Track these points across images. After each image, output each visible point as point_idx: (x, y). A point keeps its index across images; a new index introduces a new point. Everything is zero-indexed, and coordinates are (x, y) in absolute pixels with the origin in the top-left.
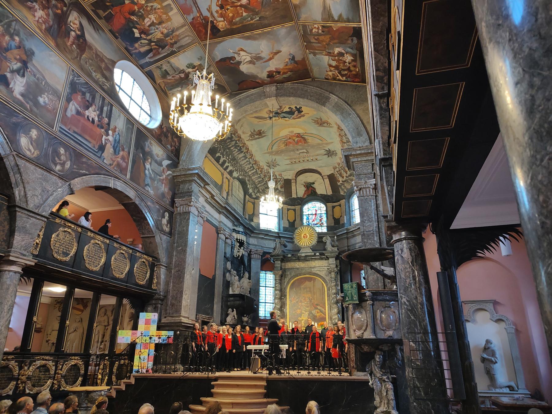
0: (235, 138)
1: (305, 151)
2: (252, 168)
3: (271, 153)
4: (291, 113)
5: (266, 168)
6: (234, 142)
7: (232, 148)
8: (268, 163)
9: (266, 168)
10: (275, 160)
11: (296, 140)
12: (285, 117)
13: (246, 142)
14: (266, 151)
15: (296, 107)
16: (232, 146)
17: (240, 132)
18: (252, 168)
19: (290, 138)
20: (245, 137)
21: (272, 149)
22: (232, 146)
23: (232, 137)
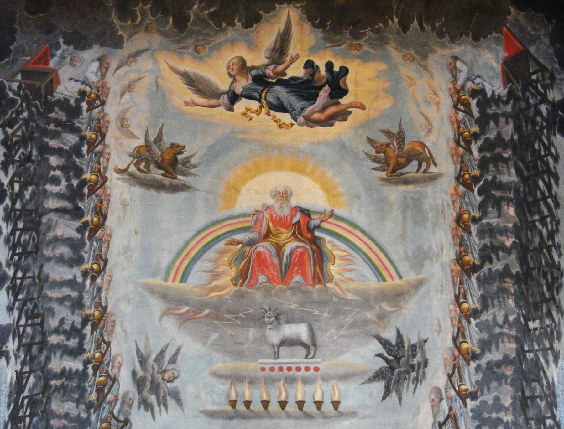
0: (82, 122)
1: (301, 331)
2: (73, 343)
3: (172, 301)
4: (305, 89)
5: (125, 384)
6: (71, 139)
7: (54, 160)
8: (143, 361)
9: (125, 384)
10: (173, 360)
11: (287, 249)
12: (281, 108)
13: (111, 175)
14: (158, 281)
15: (329, 66)
16: (59, 152)
17: (112, 109)
18: (73, 343)
19: (267, 235)
20: (119, 151)
21: (184, 279)
22: (59, 152)
23: (74, 112)
